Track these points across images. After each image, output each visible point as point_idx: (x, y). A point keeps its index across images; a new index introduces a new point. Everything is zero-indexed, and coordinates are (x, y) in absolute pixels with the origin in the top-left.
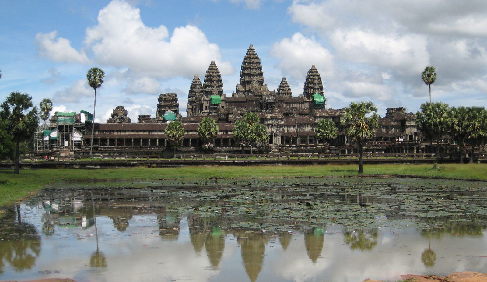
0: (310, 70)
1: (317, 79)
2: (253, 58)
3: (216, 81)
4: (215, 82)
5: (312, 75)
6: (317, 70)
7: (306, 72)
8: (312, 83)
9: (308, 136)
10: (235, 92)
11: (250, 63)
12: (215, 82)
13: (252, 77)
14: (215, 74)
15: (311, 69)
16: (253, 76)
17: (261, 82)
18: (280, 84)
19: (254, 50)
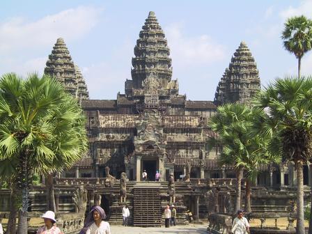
0: (237, 50)
1: (246, 67)
2: (153, 35)
3: (61, 73)
4: (58, 74)
5: (239, 60)
6: (250, 52)
7: (231, 55)
8: (237, 74)
9: (78, 168)
10: (123, 92)
11: (146, 43)
12: (58, 74)
13: (146, 68)
14: (59, 60)
15: (237, 48)
16: (150, 64)
17: (166, 76)
18: (222, 79)
19: (156, 20)
